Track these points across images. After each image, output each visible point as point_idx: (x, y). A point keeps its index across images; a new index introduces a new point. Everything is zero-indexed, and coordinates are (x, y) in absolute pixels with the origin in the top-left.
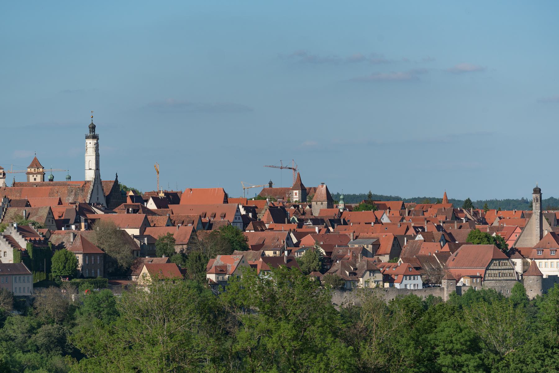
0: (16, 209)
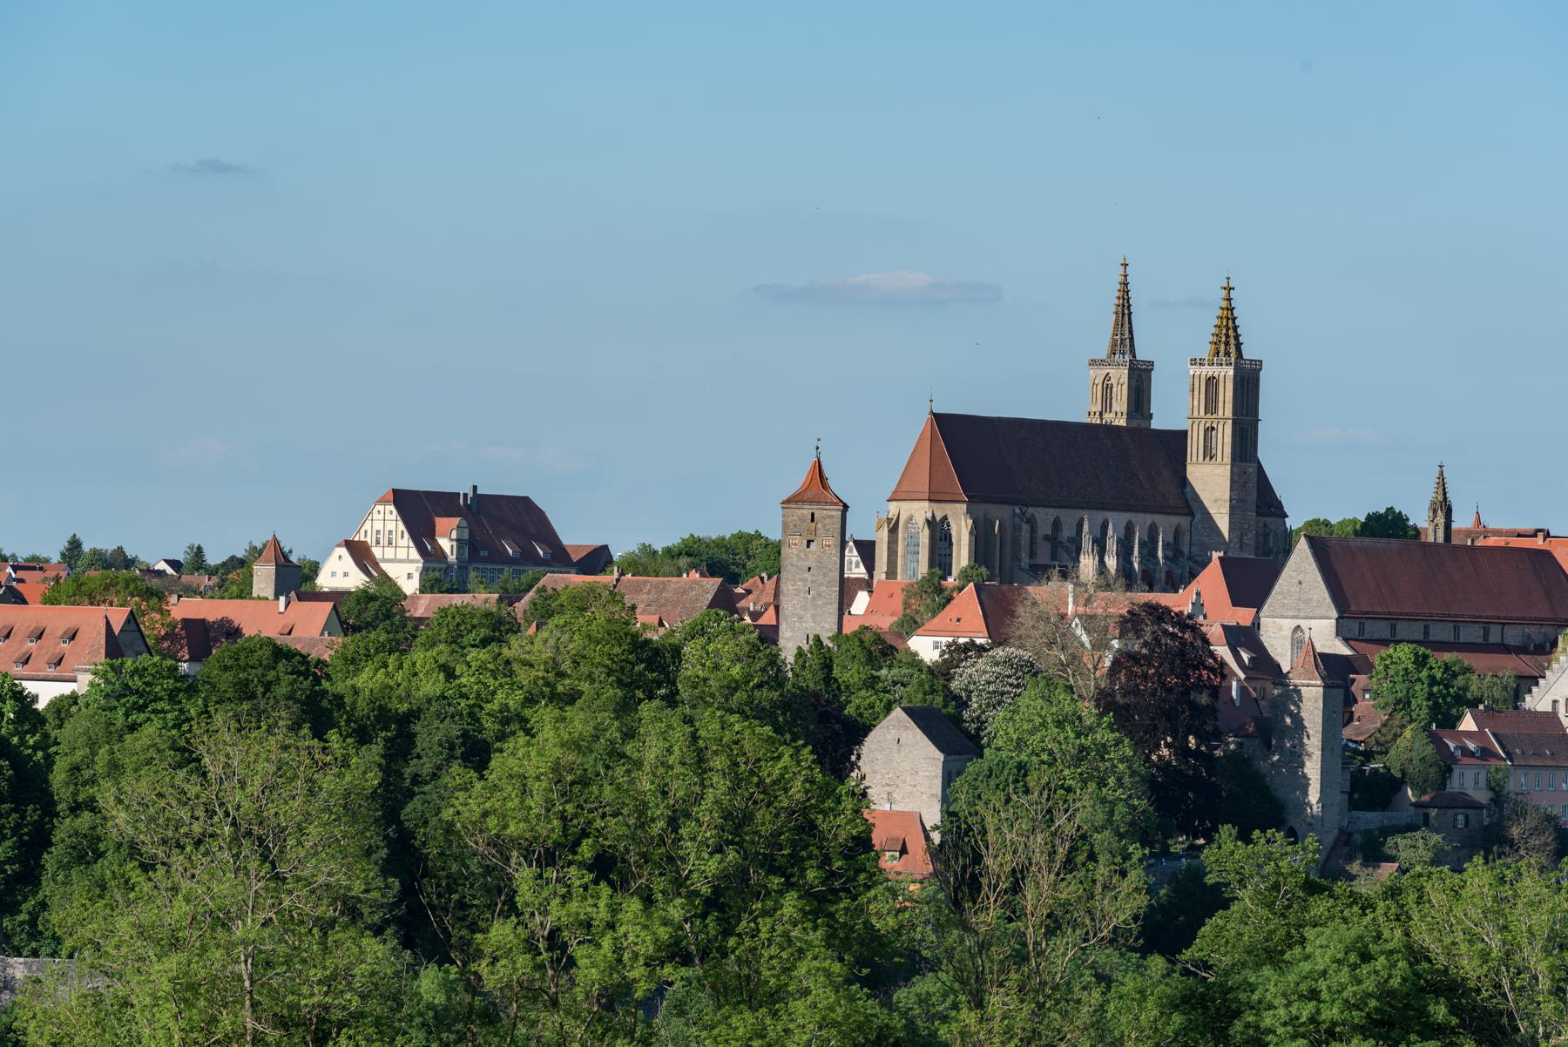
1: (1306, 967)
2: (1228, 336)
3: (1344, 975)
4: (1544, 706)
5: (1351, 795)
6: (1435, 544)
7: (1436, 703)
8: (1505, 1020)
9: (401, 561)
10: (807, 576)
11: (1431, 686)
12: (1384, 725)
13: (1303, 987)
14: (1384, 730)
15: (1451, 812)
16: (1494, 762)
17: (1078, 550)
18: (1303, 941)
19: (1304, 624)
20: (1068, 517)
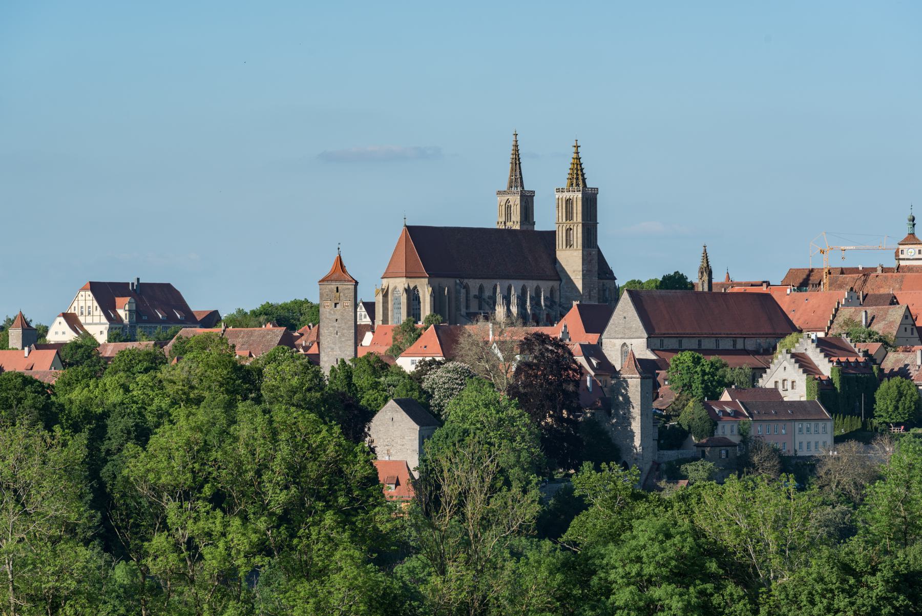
0: (852, 309)
1: (634, 543)
2: (578, 174)
3: (656, 547)
4: (770, 385)
5: (659, 441)
6: (703, 292)
7: (707, 386)
8: (751, 570)
9: (96, 324)
10: (336, 324)
11: (703, 376)
12: (677, 399)
13: (632, 555)
14: (677, 403)
15: (718, 449)
16: (742, 419)
17: (495, 303)
18: (631, 528)
19: (628, 342)
20: (488, 284)
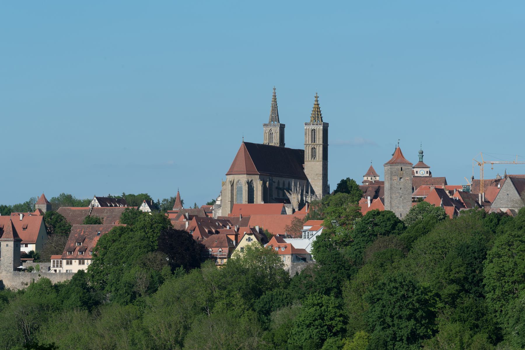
2: (317, 114)
